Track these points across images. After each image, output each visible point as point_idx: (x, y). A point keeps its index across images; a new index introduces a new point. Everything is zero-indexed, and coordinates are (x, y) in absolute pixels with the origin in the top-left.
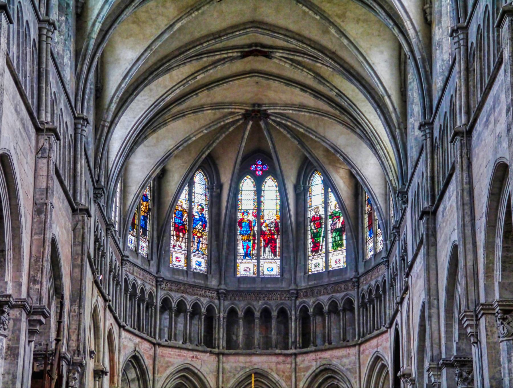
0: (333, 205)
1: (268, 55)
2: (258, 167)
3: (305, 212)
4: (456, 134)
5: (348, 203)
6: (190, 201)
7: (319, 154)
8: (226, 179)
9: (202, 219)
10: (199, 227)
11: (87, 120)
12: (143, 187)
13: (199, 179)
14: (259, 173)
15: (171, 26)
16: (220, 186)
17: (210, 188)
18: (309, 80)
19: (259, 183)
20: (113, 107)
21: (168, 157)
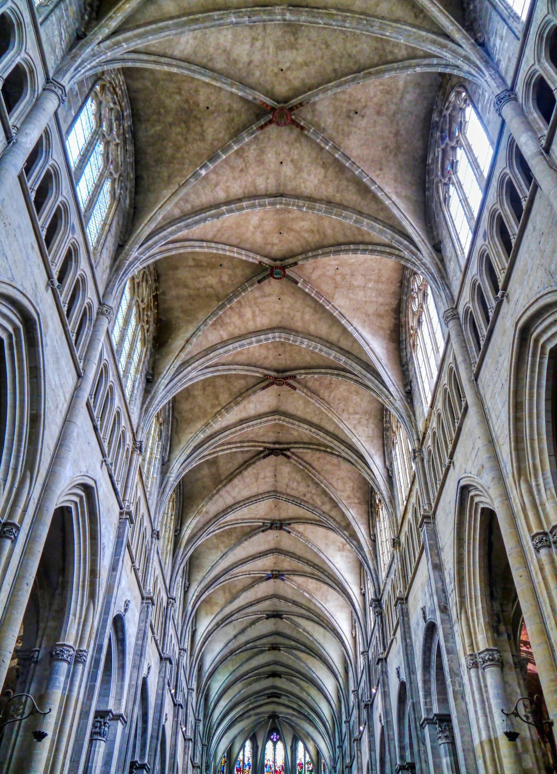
0: (308, 759)
1: (279, 697)
2: (274, 736)
3: (295, 760)
4: (346, 767)
5: (314, 758)
6: (244, 755)
7: (301, 735)
8: (260, 744)
9: (249, 764)
10: (247, 769)
11: (193, 690)
12: (224, 753)
13: (248, 744)
14: (275, 740)
15: (240, 692)
16: (257, 747)
17: (253, 748)
18: (295, 706)
19: (275, 744)
20: (215, 727)
21: (235, 738)
